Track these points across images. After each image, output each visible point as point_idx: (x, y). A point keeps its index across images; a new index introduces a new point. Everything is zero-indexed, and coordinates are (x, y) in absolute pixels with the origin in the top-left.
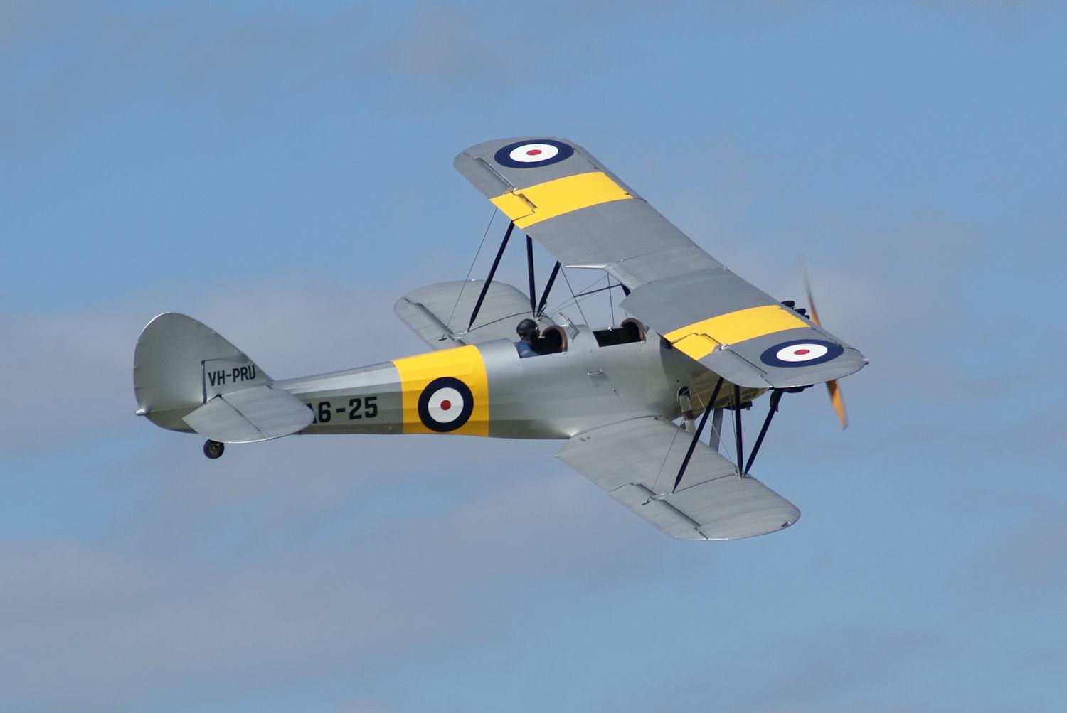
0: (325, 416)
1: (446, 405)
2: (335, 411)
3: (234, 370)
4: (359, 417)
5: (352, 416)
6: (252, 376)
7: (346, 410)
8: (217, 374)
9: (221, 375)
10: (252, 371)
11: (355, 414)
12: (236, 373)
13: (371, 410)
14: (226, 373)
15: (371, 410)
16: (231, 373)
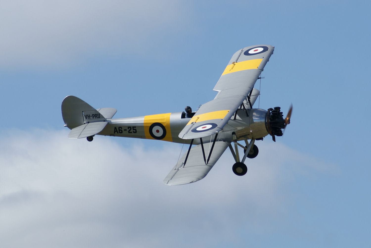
0: (121, 131)
1: (158, 131)
2: (124, 130)
3: (93, 115)
4: (131, 133)
5: (129, 132)
6: (99, 117)
7: (127, 130)
8: (87, 116)
9: (89, 116)
10: (99, 115)
11: (130, 132)
12: (93, 116)
13: (135, 131)
14: (90, 115)
15: (135, 131)
16: (92, 115)
